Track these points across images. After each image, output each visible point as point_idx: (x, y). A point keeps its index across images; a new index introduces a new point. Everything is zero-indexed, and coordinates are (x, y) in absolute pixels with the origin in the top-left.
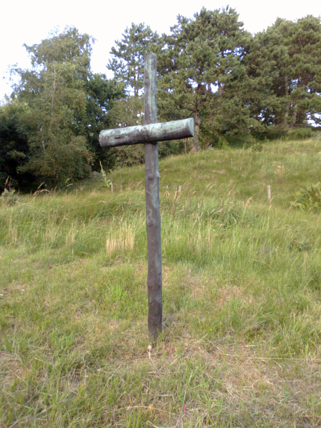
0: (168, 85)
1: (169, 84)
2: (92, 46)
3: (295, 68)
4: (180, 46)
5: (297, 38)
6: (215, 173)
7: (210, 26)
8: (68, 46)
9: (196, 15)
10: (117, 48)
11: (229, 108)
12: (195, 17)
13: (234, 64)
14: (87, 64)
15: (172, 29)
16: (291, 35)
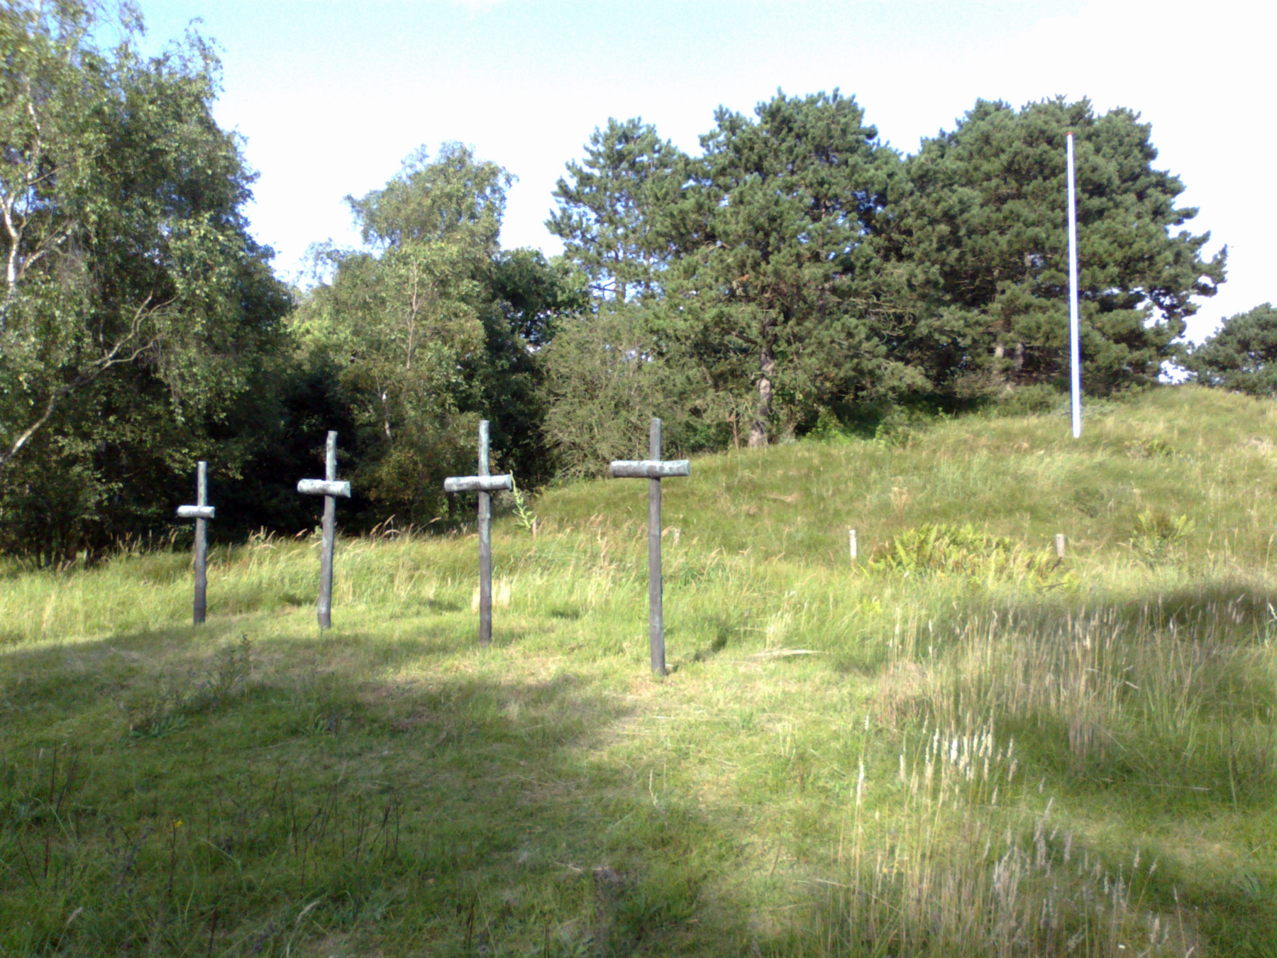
0: (688, 284)
1: (693, 279)
3: (1007, 237)
4: (718, 186)
5: (1011, 163)
6: (775, 500)
7: (791, 141)
8: (450, 196)
9: (761, 110)
10: (572, 184)
11: (832, 342)
13: (841, 238)
14: (492, 236)
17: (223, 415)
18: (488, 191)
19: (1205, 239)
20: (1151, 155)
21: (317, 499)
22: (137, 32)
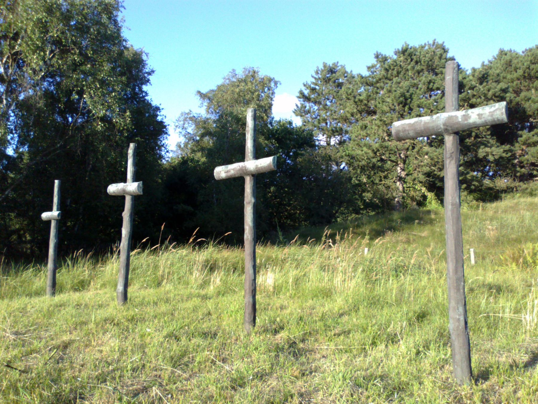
0: (363, 133)
2: (275, 91)
4: (378, 88)
12: (396, 54)
15: (369, 68)
16: (516, 70)
18: (266, 89)
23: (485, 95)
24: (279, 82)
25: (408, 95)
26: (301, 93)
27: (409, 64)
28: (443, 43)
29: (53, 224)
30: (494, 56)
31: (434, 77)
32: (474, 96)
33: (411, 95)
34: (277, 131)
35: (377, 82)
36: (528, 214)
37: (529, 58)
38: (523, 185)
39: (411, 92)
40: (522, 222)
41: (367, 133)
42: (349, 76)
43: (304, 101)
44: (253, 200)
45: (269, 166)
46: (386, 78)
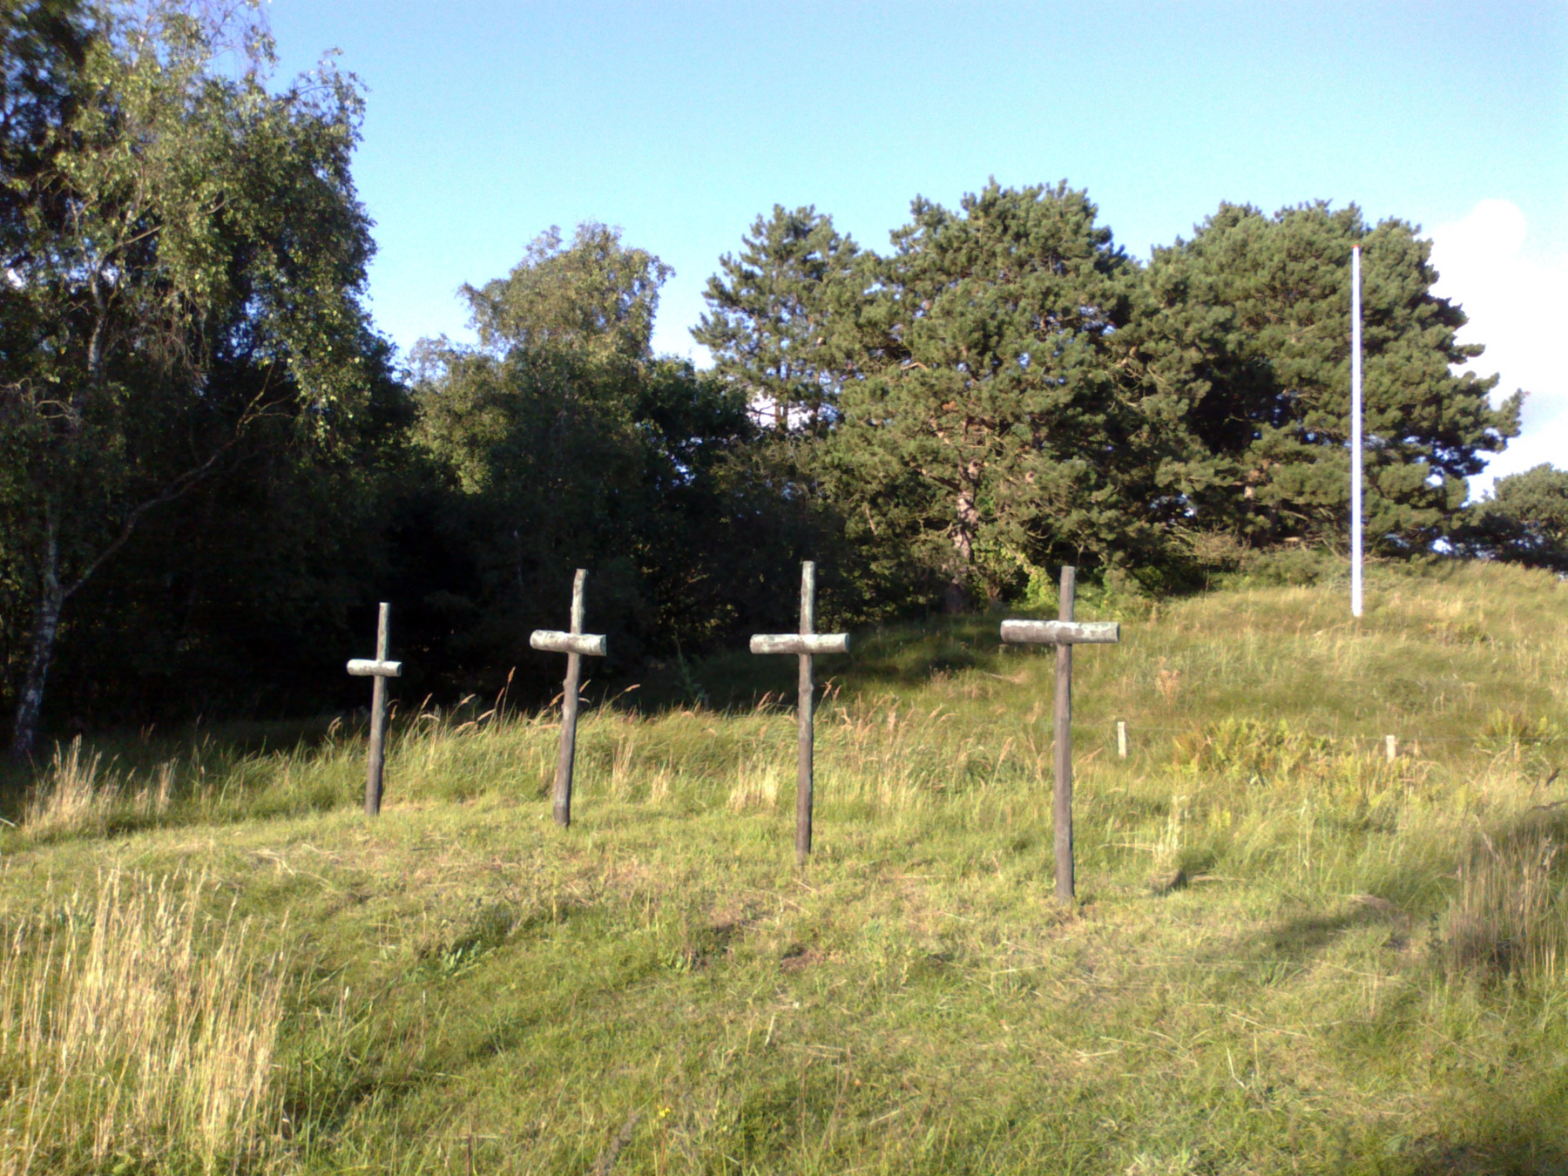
0: (878, 409)
2: (660, 291)
9: (968, 203)
12: (965, 208)
15: (896, 236)
16: (1256, 266)
17: (336, 548)
19: (1494, 381)
20: (1434, 278)
21: (557, 660)
22: (264, 61)
23: (1179, 335)
24: (669, 268)
25: (992, 325)
26: (715, 284)
27: (1000, 240)
28: (1085, 191)
29: (378, 685)
30: (1207, 217)
31: (1058, 279)
32: (1151, 333)
33: (999, 327)
34: (656, 391)
35: (917, 277)
36: (1251, 637)
37: (1286, 243)
38: (1259, 557)
39: (1000, 317)
40: (1238, 659)
41: (887, 412)
42: (841, 248)
43: (721, 306)
44: (812, 688)
45: (839, 647)
46: (941, 269)
